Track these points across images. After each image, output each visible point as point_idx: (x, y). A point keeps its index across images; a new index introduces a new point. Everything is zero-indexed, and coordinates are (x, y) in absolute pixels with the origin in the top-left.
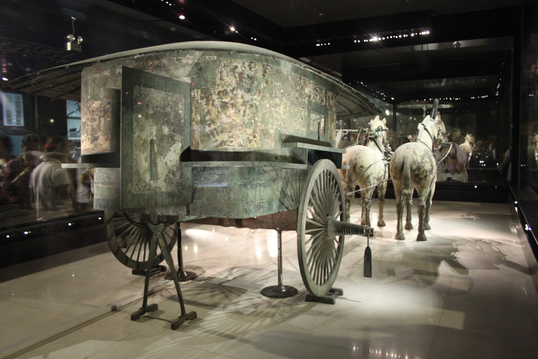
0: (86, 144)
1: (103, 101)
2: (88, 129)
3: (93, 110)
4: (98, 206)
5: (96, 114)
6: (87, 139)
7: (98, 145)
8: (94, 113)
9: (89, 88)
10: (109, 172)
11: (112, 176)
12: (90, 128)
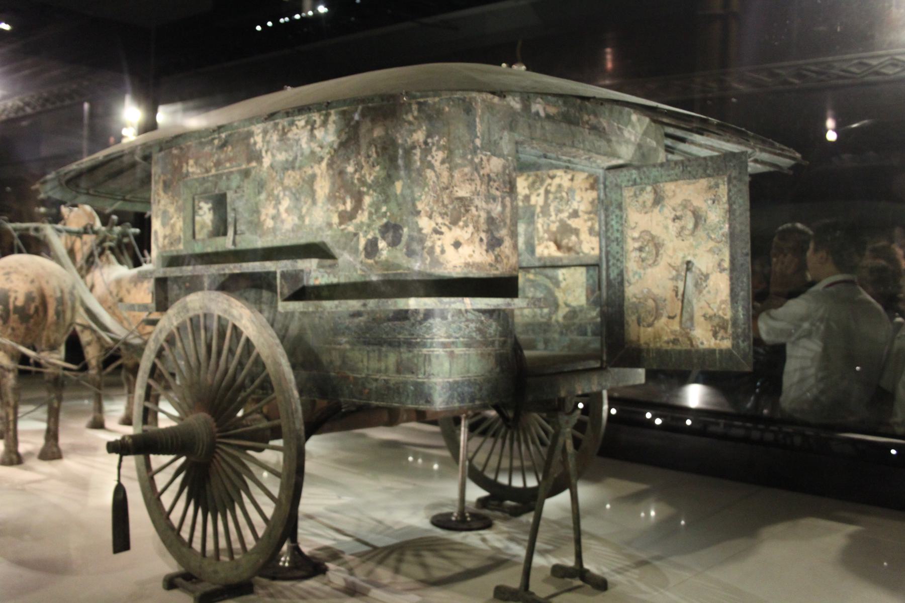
0: (474, 251)
1: (507, 160)
2: (479, 216)
3: (488, 175)
4: (455, 401)
5: (496, 185)
6: (477, 240)
7: (503, 257)
8: (491, 183)
9: (478, 120)
10: (483, 318)
11: (490, 326)
12: (483, 215)
